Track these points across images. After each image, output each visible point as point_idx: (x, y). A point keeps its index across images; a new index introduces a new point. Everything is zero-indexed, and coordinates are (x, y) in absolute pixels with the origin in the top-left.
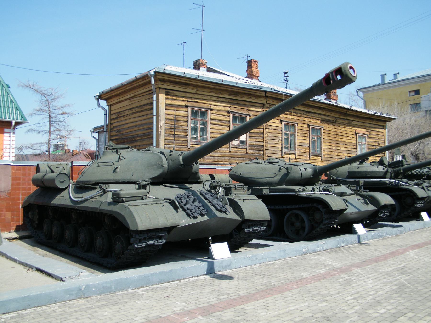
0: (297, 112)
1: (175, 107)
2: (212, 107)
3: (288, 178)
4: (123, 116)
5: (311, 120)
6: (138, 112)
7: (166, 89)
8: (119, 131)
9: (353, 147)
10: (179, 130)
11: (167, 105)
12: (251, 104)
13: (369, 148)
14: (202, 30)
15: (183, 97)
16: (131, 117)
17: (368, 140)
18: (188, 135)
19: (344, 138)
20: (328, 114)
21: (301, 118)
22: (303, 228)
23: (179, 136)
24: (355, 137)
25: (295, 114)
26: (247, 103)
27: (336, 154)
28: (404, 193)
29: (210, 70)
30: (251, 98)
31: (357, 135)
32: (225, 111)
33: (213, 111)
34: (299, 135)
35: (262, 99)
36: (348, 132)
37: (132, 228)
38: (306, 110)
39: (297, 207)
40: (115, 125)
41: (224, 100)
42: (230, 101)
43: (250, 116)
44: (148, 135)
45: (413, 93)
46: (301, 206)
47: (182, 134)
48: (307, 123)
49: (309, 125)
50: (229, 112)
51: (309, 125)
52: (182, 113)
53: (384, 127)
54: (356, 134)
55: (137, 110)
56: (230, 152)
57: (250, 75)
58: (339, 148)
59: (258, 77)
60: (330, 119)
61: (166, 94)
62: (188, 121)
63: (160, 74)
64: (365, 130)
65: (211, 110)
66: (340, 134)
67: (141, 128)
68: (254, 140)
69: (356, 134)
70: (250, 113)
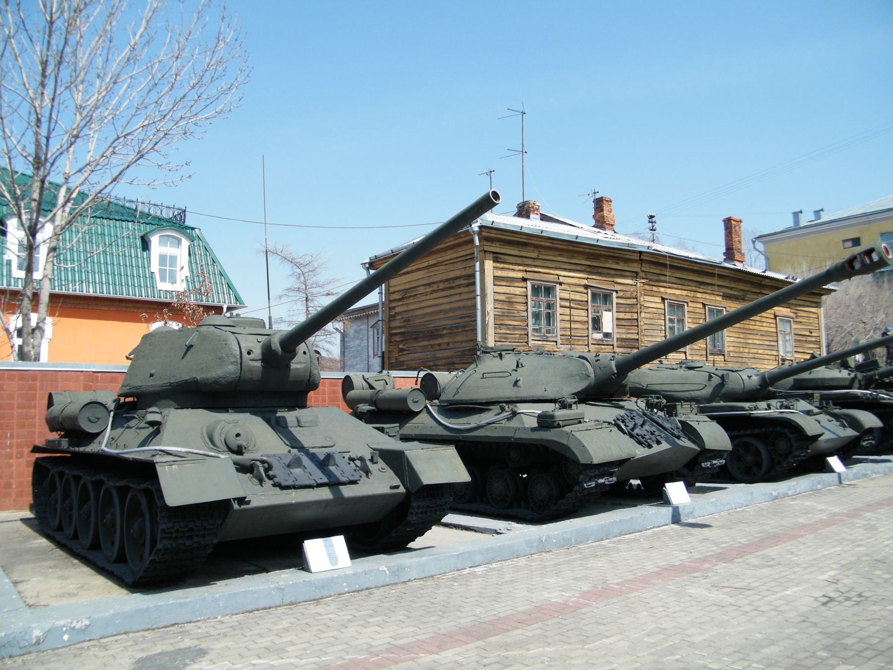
0: (687, 283)
1: (507, 281)
2: (561, 279)
3: (724, 390)
4: (415, 296)
5: (708, 297)
6: (443, 290)
7: (494, 253)
8: (407, 320)
9: (771, 339)
10: (514, 318)
11: (496, 278)
12: (619, 273)
13: (796, 341)
14: (523, 152)
15: (519, 265)
16: (428, 297)
17: (794, 326)
18: (527, 325)
19: (758, 324)
20: (732, 285)
21: (692, 294)
22: (759, 465)
23: (515, 328)
24: (773, 321)
25: (684, 287)
26: (613, 272)
27: (747, 350)
28: (888, 410)
29: (544, 218)
30: (618, 263)
32: (580, 285)
33: (563, 287)
34: (690, 320)
35: (635, 265)
37: (583, 460)
38: (699, 279)
39: (749, 432)
40: (397, 310)
41: (578, 268)
42: (588, 270)
43: (617, 292)
44: (464, 327)
45: (849, 244)
46: (756, 431)
47: (519, 323)
48: (701, 300)
49: (704, 305)
50: (586, 287)
51: (704, 305)
52: (518, 291)
53: (818, 305)
55: (441, 286)
56: (589, 351)
57: (601, 223)
58: (751, 341)
59: (612, 225)
60: (736, 293)
61: (494, 261)
62: (527, 303)
63: (487, 230)
64: (789, 310)
65: (561, 284)
67: (451, 314)
68: (623, 331)
69: (776, 316)
70: (617, 287)
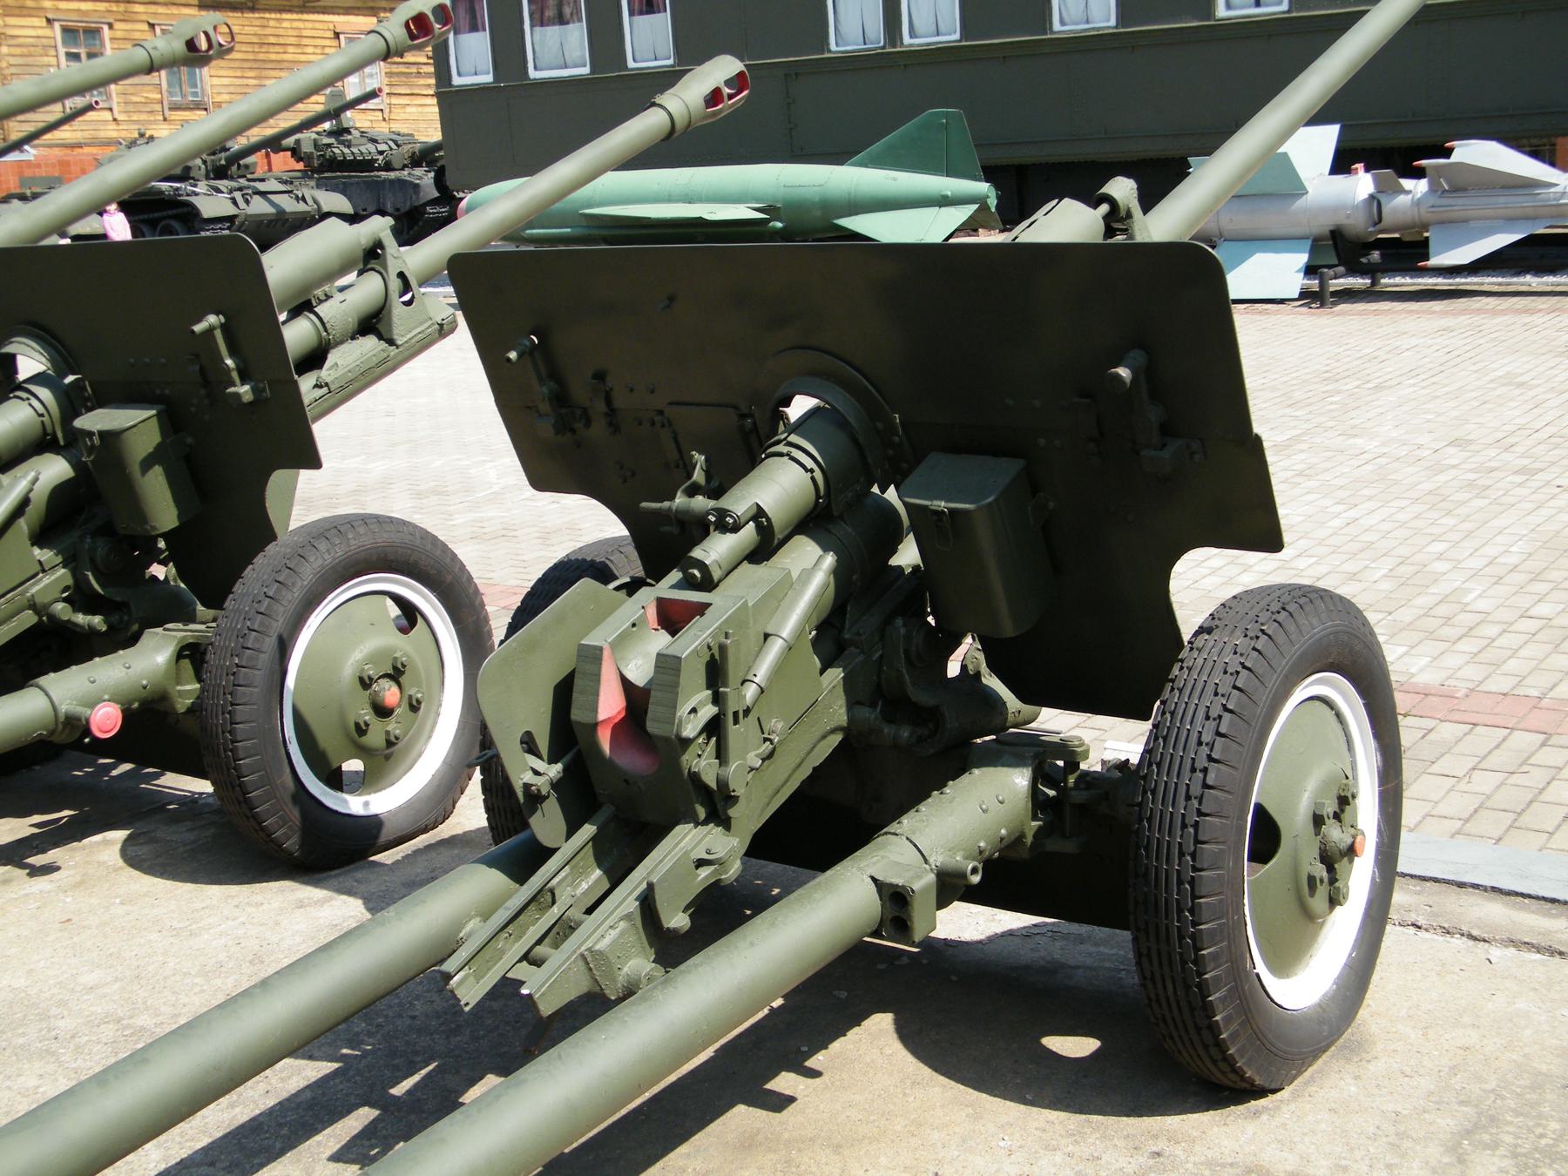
5: (161, 10)
19: (291, 49)
24: (335, 43)
31: (342, 37)
36: (306, 33)
48: (144, 17)
51: (152, 26)
54: (337, 35)
64: (374, 20)
66: (272, 40)
69: (337, 35)
